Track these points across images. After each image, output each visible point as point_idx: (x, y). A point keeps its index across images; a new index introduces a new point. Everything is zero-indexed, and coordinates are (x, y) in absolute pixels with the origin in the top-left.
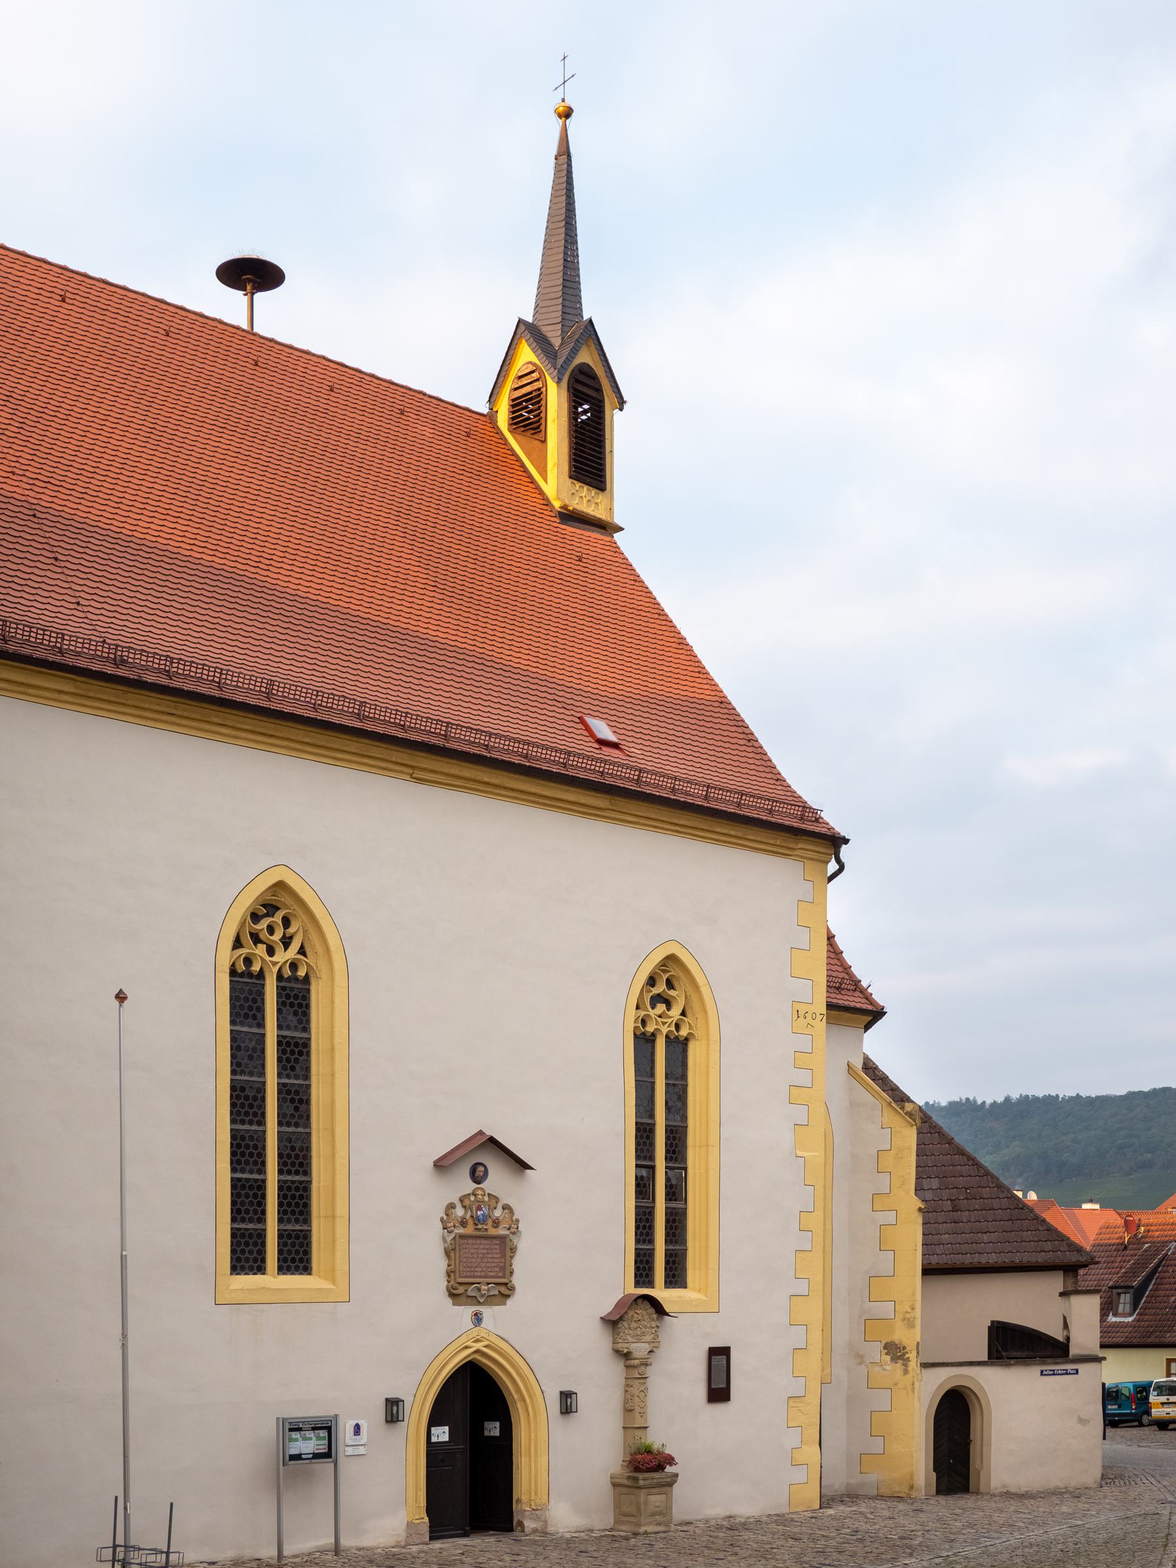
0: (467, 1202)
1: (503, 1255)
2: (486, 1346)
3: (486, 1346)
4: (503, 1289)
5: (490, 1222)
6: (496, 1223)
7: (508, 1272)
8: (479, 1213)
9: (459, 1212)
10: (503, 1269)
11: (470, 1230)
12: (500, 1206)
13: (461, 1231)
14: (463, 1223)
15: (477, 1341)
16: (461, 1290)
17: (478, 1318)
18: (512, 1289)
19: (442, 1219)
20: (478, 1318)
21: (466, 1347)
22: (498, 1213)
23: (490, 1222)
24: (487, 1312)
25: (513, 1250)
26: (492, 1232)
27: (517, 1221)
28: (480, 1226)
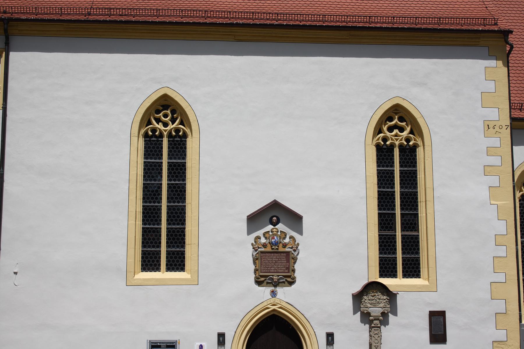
0: (267, 235)
1: (288, 261)
2: (280, 308)
3: (280, 308)
4: (289, 279)
5: (281, 245)
6: (285, 246)
7: (291, 270)
8: (273, 240)
9: (263, 240)
10: (288, 268)
11: (269, 249)
12: (288, 237)
13: (263, 249)
14: (265, 245)
15: (274, 305)
16: (262, 279)
17: (274, 294)
18: (294, 278)
19: (252, 244)
20: (274, 294)
21: (268, 308)
22: (287, 240)
23: (281, 245)
24: (280, 290)
25: (295, 260)
26: (281, 249)
27: (298, 244)
28: (273, 247)
